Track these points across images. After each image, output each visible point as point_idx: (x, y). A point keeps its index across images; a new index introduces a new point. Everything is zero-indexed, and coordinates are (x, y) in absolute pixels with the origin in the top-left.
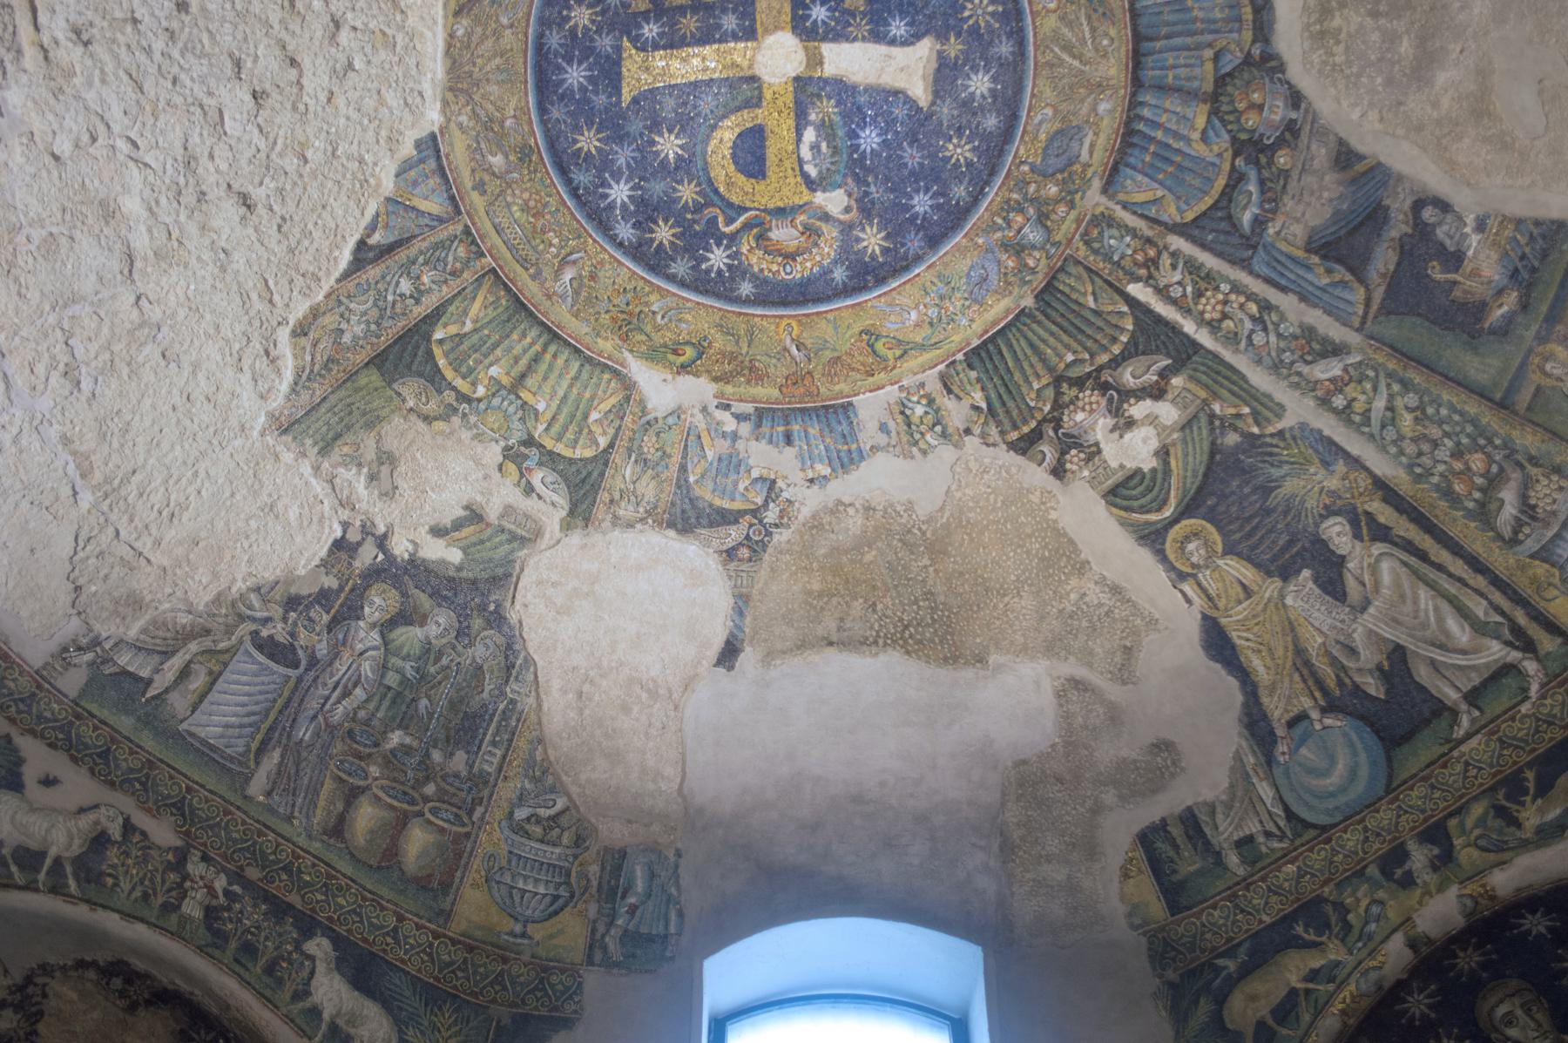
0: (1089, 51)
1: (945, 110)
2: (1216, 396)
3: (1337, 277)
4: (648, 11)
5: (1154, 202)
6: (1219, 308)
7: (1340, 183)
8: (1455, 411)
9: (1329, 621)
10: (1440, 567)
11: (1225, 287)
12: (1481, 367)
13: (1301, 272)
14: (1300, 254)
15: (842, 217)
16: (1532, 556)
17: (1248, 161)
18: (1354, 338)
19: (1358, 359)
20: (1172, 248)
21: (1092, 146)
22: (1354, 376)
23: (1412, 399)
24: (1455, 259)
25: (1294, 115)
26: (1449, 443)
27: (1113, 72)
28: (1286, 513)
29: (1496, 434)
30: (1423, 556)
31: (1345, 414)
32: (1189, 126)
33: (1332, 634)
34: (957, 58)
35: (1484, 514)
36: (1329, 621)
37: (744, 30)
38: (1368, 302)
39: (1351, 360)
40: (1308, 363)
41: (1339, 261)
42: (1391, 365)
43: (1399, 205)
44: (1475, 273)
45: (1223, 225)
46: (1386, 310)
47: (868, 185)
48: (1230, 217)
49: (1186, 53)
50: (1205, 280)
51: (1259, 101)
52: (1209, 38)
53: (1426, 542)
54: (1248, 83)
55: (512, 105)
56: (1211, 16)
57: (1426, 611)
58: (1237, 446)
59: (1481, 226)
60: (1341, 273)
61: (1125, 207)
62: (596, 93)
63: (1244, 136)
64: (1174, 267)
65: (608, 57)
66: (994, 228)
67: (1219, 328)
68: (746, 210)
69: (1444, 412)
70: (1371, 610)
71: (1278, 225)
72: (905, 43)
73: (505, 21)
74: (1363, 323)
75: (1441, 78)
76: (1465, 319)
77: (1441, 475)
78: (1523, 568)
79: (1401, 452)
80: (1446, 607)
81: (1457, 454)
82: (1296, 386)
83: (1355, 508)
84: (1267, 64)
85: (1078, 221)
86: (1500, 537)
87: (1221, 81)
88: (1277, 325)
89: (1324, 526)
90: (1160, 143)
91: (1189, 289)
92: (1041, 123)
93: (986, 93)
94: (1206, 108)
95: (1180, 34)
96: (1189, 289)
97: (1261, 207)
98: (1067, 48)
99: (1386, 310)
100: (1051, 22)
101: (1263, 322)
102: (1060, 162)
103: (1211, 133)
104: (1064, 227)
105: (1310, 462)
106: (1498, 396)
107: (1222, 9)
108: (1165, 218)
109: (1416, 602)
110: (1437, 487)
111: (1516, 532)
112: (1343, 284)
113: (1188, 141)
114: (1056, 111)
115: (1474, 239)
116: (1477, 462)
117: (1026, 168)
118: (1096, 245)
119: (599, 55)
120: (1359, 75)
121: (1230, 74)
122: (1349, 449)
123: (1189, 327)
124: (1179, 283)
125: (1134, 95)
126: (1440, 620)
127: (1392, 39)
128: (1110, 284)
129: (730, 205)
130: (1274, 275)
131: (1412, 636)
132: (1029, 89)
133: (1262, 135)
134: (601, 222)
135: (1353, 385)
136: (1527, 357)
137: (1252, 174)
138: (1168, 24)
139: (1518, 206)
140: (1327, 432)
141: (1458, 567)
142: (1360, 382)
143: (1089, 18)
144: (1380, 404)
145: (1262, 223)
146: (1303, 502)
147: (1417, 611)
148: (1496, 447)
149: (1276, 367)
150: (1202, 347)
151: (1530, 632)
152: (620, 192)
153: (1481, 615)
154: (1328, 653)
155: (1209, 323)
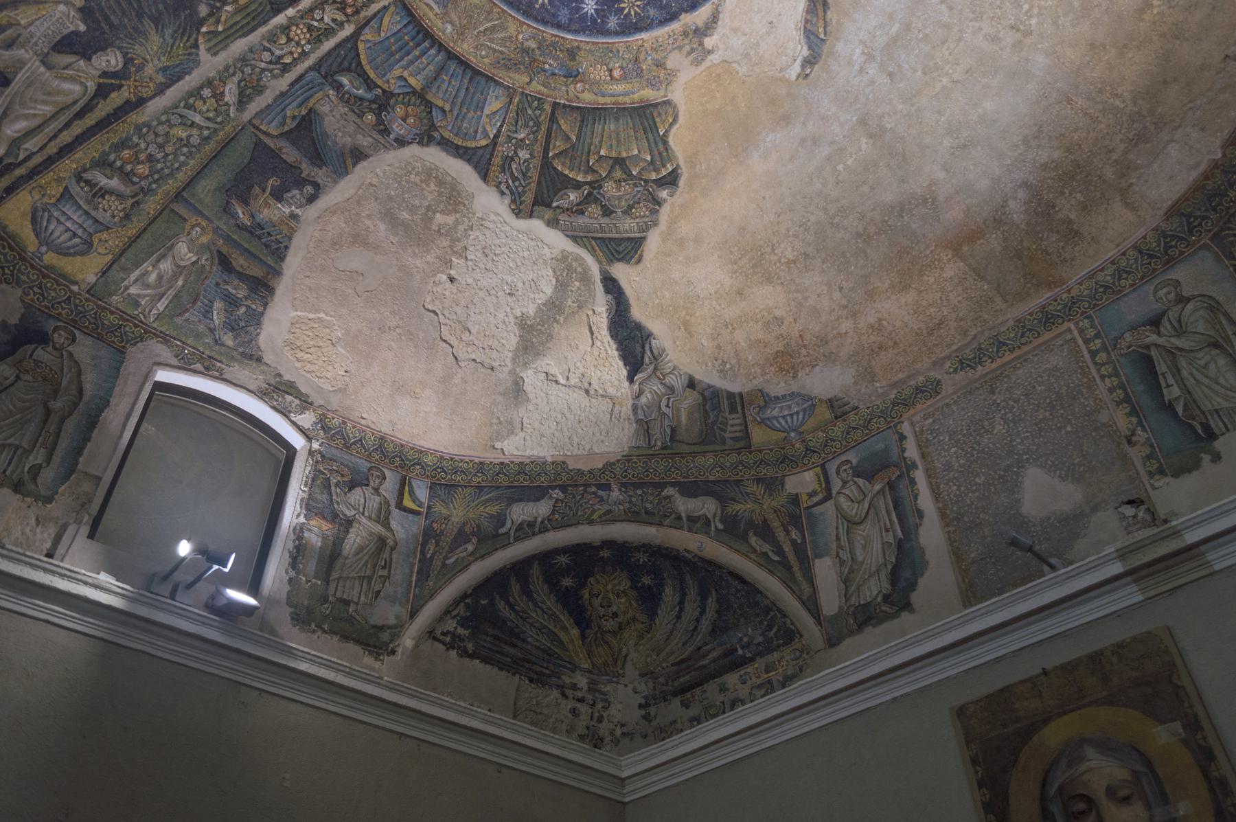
0: (482, 40)
2: (238, 10)
5: (379, 28)
6: (296, 38)
7: (344, 145)
9: (38, 34)
10: (68, 125)
12: (206, 188)
14: (311, 103)
16: (66, 188)
18: (246, 116)
23: (195, 140)
24: (278, 195)
26: (160, 156)
27: (465, 46)
28: (135, 29)
29: (159, 187)
30: (79, 115)
31: (196, 93)
32: (411, 73)
33: (25, 33)
35: (103, 163)
36: (38, 34)
40: (239, 82)
41: (297, 127)
43: (321, 175)
44: (267, 205)
45: (346, 64)
46: (259, 144)
48: (349, 70)
50: (318, 37)
52: (455, 113)
53: (90, 120)
57: (35, 108)
58: (197, 12)
59: (294, 216)
61: (385, 7)
63: (392, 101)
64: (334, 20)
67: (283, 33)
69: (182, 158)
70: (42, 69)
71: (333, 98)
74: (254, 126)
75: (382, 227)
76: (240, 189)
77: (138, 144)
78: (59, 180)
79: (161, 123)
80: (37, 122)
81: (150, 158)
82: (227, 69)
83: (126, 79)
84: (427, 137)
86: (85, 170)
87: (429, 105)
88: (271, 71)
89: (118, 53)
91: (316, 24)
94: (418, 87)
95: (465, 98)
96: (316, 24)
97: (347, 92)
98: (493, 29)
99: (259, 144)
100: (512, 30)
101: (276, 63)
103: (403, 83)
105: (169, 59)
106: (185, 194)
108: (367, 30)
109: (43, 102)
110: (129, 139)
111: (87, 182)
112: (283, 124)
113: (405, 68)
115: (287, 210)
116: (142, 169)
120: (399, 183)
121: (430, 112)
122: (172, 89)
123: (291, 12)
124: (322, 19)
126: (26, 117)
127: (412, 210)
130: (303, 82)
131: (15, 94)
136: (208, 219)
137: (369, 96)
138: (474, 93)
139: (299, 240)
140: (187, 78)
141: (66, 137)
143: (501, 53)
144: (198, 119)
146: (141, 44)
147: (36, 101)
148: (150, 184)
149: (243, 60)
150: (275, 16)
151: (7, 177)
153: (26, 146)
154: (10, 25)
155: (288, 27)
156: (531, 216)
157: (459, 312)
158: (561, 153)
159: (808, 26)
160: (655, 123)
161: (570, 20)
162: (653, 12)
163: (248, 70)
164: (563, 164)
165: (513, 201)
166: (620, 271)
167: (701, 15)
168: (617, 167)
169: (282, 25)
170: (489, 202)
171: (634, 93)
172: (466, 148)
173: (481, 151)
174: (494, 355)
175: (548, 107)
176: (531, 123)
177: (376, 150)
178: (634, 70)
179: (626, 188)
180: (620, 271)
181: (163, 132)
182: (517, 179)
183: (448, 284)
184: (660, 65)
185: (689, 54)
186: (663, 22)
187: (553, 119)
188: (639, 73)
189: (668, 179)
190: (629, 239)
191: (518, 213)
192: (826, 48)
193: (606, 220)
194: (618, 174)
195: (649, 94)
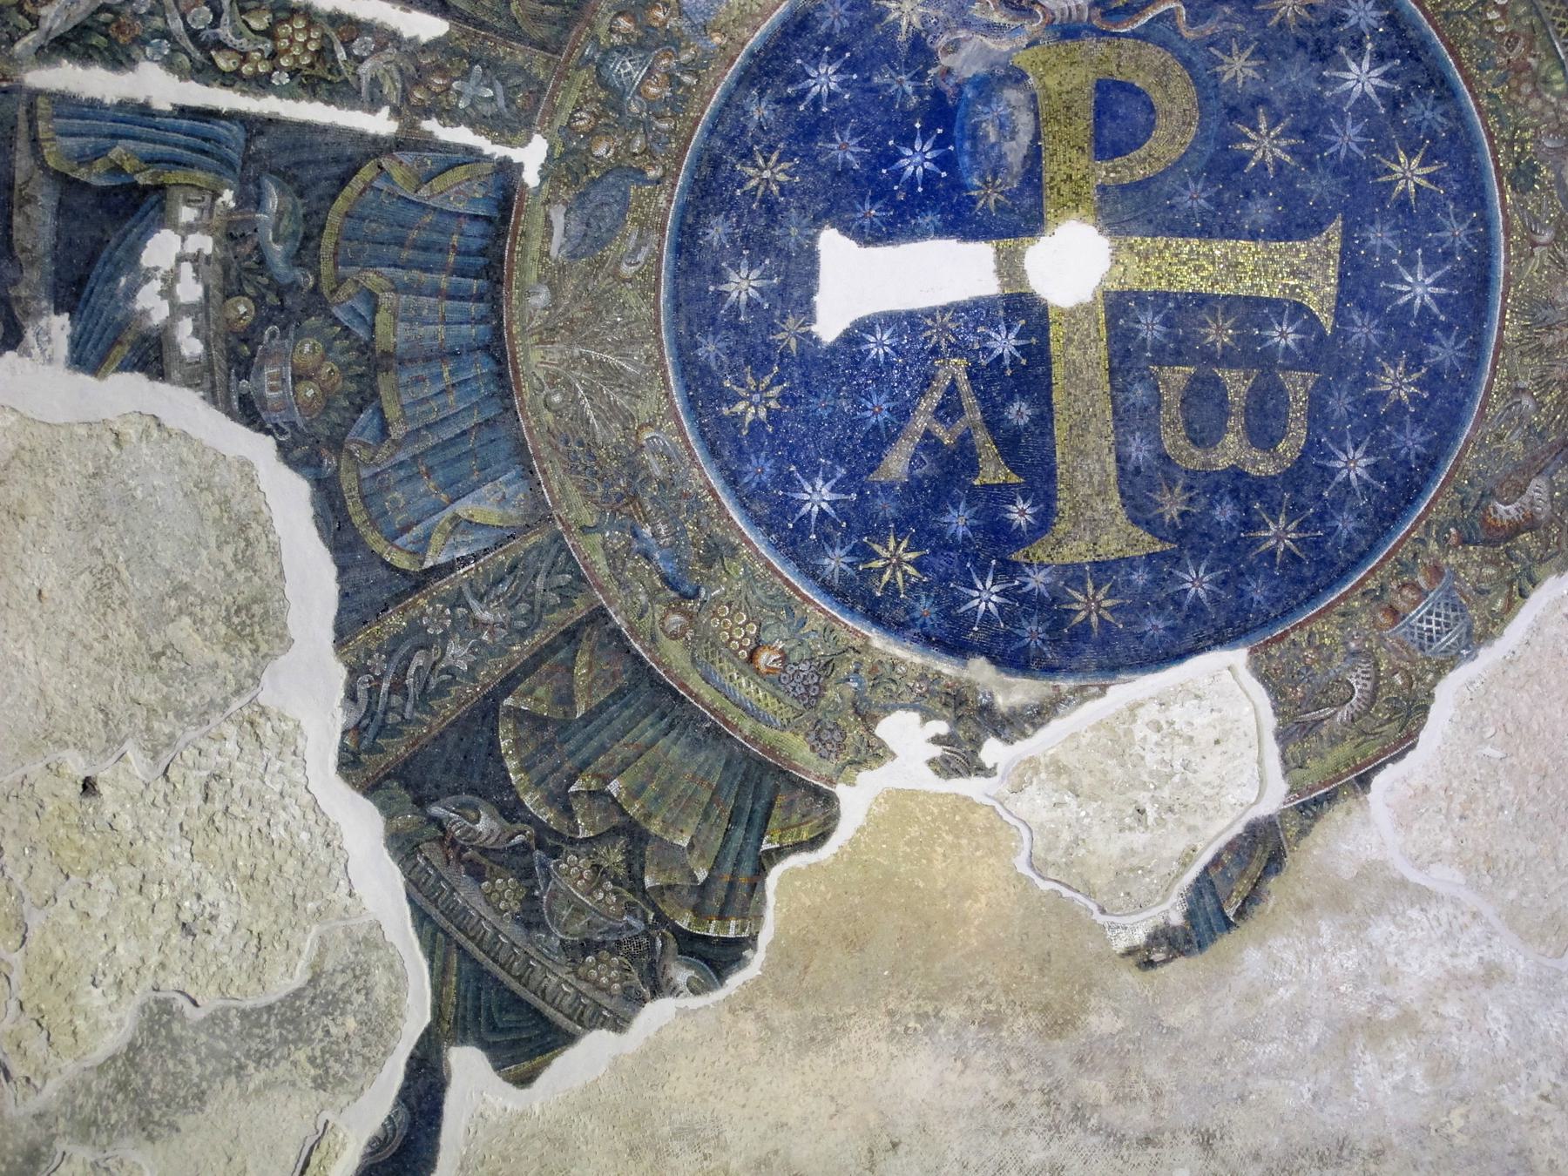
1: (794, 231)
3: (100, 166)
4: (1285, 369)
5: (431, 177)
6: (284, 43)
13: (160, 148)
15: (962, 34)
17: (294, 287)
19: (18, 47)
20: (385, 111)
21: (550, 235)
25: (244, 383)
27: (536, 356)
34: (784, 317)
37: (1126, 311)
38: (35, 141)
39: (31, 40)
41: (104, 192)
45: (310, 173)
47: (918, 91)
49: (432, 417)
51: (301, 386)
54: (327, 407)
55: (1535, 263)
56: (408, 487)
60: (96, 176)
62: (1385, 248)
64: (375, 82)
65: (1362, 307)
66: (693, 68)
67: (273, 11)
68: (1134, 35)
72: (866, 326)
73: (1526, 401)
74: (31, 108)
85: (554, 110)
87: (366, 398)
88: (176, 49)
90: (443, 269)
91: (341, 55)
92: (637, 250)
93: (734, 277)
100: (644, 410)
101: (203, 47)
102: (597, 196)
103: (362, 309)
104: (575, 94)
107: (394, 501)
108: (407, 158)
112: (85, 159)
113: (398, 288)
114: (615, 275)
117: (652, 174)
118: (518, 80)
119: (1378, 311)
124: (361, 60)
125: (497, 332)
128: (481, 25)
129: (1164, 44)
132: (663, 296)
133: (284, 336)
134: (1401, 33)
143: (590, 432)
145: (246, 203)
152: (1361, 78)
156: (370, 789)
157: (40, 873)
158: (532, 716)
159: (1213, 873)
160: (767, 817)
161: (761, 486)
162: (925, 608)
164: (518, 743)
165: (355, 731)
166: (468, 1066)
167: (1015, 693)
168: (622, 842)
170: (310, 693)
171: (769, 724)
172: (357, 542)
173: (383, 573)
174: (35, 1044)
175: (581, 608)
176: (523, 608)
177: (190, 382)
178: (807, 685)
179: (606, 896)
180: (468, 1066)
182: (406, 696)
183: (72, 791)
184: (867, 716)
185: (937, 740)
186: (928, 640)
187: (571, 635)
188: (811, 697)
189: (713, 952)
190: (537, 1012)
191: (349, 763)
192: (1226, 942)
193: (511, 931)
194: (614, 856)
195: (799, 751)
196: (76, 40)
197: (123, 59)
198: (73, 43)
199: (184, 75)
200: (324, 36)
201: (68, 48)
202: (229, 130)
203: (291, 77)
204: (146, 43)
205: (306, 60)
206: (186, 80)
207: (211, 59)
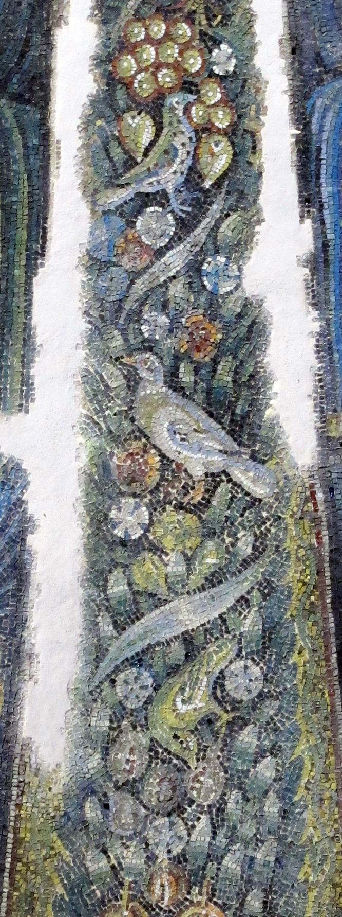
6: (166, 77)
8: (286, 794)
11: (223, 58)
19: (259, 491)
22: (207, 504)
23: (245, 680)
31: (108, 550)
40: (172, 380)
42: (293, 576)
67: (119, 118)
69: (266, 769)
82: (97, 391)
101: (201, 204)
135: (190, 521)
142: (212, 534)
144: (189, 614)
149: (111, 314)
163: (155, 323)
169: (94, 102)
181: (139, 761)
196: (231, 407)
197: (246, 322)
198: (237, 412)
199: (251, 222)
200: (138, 17)
201: (245, 417)
202: (326, 109)
203: (217, 43)
204: (214, 294)
205: (184, 30)
206: (259, 211)
207: (218, 184)
